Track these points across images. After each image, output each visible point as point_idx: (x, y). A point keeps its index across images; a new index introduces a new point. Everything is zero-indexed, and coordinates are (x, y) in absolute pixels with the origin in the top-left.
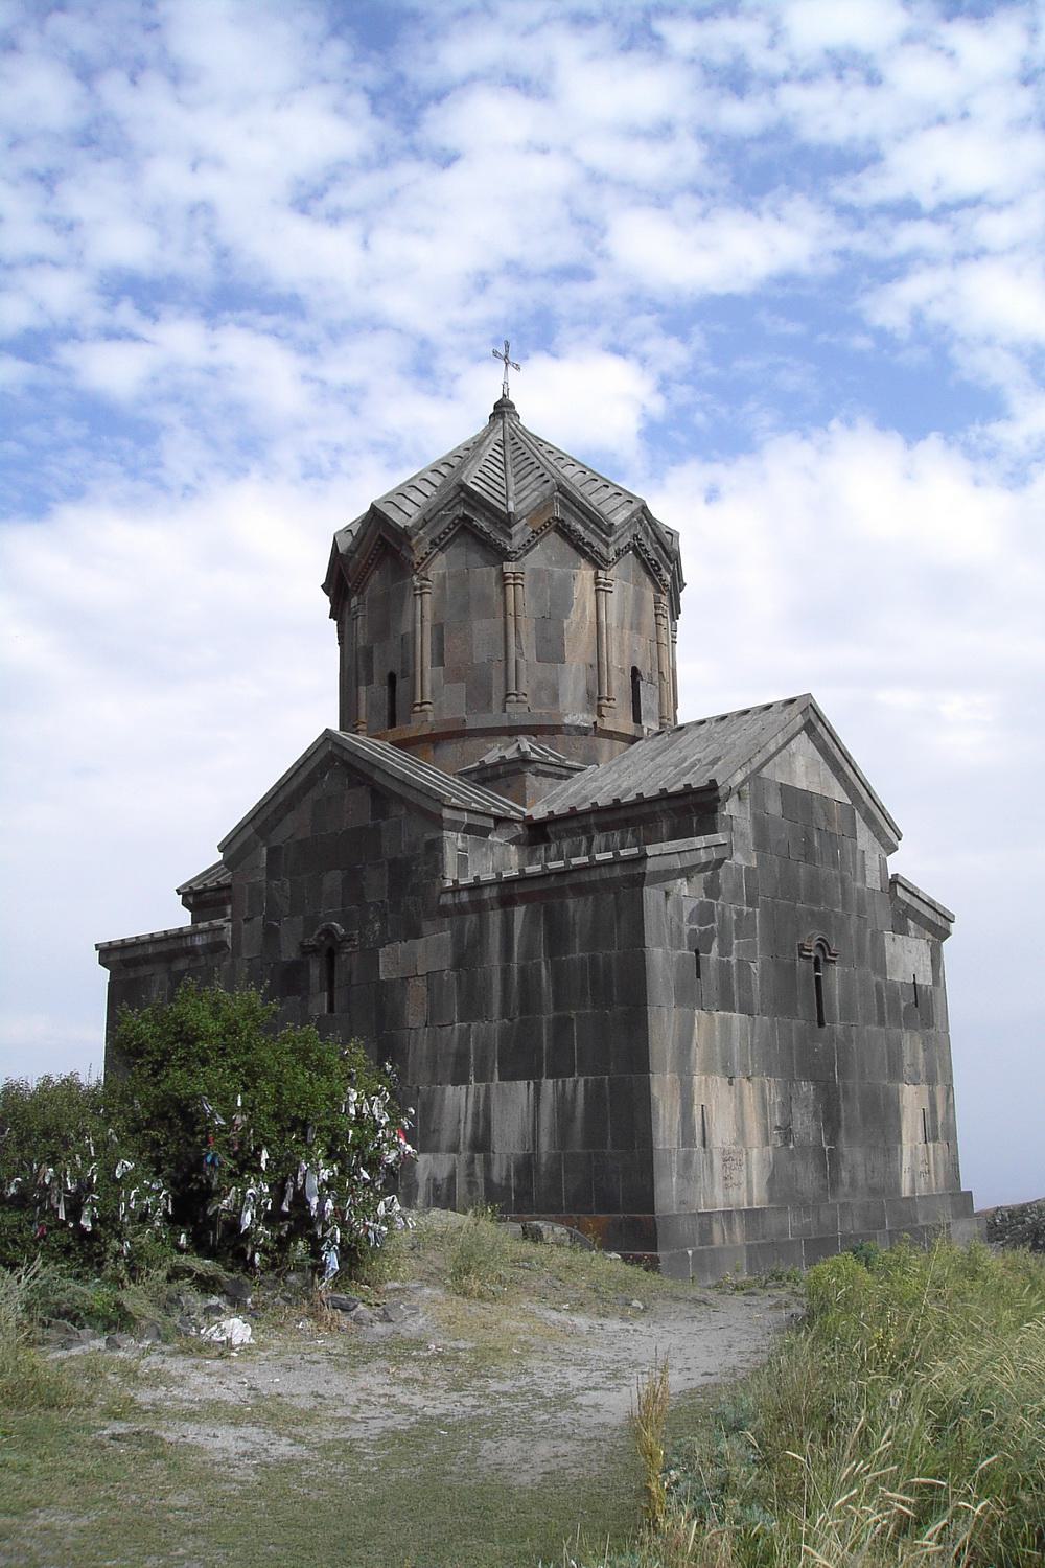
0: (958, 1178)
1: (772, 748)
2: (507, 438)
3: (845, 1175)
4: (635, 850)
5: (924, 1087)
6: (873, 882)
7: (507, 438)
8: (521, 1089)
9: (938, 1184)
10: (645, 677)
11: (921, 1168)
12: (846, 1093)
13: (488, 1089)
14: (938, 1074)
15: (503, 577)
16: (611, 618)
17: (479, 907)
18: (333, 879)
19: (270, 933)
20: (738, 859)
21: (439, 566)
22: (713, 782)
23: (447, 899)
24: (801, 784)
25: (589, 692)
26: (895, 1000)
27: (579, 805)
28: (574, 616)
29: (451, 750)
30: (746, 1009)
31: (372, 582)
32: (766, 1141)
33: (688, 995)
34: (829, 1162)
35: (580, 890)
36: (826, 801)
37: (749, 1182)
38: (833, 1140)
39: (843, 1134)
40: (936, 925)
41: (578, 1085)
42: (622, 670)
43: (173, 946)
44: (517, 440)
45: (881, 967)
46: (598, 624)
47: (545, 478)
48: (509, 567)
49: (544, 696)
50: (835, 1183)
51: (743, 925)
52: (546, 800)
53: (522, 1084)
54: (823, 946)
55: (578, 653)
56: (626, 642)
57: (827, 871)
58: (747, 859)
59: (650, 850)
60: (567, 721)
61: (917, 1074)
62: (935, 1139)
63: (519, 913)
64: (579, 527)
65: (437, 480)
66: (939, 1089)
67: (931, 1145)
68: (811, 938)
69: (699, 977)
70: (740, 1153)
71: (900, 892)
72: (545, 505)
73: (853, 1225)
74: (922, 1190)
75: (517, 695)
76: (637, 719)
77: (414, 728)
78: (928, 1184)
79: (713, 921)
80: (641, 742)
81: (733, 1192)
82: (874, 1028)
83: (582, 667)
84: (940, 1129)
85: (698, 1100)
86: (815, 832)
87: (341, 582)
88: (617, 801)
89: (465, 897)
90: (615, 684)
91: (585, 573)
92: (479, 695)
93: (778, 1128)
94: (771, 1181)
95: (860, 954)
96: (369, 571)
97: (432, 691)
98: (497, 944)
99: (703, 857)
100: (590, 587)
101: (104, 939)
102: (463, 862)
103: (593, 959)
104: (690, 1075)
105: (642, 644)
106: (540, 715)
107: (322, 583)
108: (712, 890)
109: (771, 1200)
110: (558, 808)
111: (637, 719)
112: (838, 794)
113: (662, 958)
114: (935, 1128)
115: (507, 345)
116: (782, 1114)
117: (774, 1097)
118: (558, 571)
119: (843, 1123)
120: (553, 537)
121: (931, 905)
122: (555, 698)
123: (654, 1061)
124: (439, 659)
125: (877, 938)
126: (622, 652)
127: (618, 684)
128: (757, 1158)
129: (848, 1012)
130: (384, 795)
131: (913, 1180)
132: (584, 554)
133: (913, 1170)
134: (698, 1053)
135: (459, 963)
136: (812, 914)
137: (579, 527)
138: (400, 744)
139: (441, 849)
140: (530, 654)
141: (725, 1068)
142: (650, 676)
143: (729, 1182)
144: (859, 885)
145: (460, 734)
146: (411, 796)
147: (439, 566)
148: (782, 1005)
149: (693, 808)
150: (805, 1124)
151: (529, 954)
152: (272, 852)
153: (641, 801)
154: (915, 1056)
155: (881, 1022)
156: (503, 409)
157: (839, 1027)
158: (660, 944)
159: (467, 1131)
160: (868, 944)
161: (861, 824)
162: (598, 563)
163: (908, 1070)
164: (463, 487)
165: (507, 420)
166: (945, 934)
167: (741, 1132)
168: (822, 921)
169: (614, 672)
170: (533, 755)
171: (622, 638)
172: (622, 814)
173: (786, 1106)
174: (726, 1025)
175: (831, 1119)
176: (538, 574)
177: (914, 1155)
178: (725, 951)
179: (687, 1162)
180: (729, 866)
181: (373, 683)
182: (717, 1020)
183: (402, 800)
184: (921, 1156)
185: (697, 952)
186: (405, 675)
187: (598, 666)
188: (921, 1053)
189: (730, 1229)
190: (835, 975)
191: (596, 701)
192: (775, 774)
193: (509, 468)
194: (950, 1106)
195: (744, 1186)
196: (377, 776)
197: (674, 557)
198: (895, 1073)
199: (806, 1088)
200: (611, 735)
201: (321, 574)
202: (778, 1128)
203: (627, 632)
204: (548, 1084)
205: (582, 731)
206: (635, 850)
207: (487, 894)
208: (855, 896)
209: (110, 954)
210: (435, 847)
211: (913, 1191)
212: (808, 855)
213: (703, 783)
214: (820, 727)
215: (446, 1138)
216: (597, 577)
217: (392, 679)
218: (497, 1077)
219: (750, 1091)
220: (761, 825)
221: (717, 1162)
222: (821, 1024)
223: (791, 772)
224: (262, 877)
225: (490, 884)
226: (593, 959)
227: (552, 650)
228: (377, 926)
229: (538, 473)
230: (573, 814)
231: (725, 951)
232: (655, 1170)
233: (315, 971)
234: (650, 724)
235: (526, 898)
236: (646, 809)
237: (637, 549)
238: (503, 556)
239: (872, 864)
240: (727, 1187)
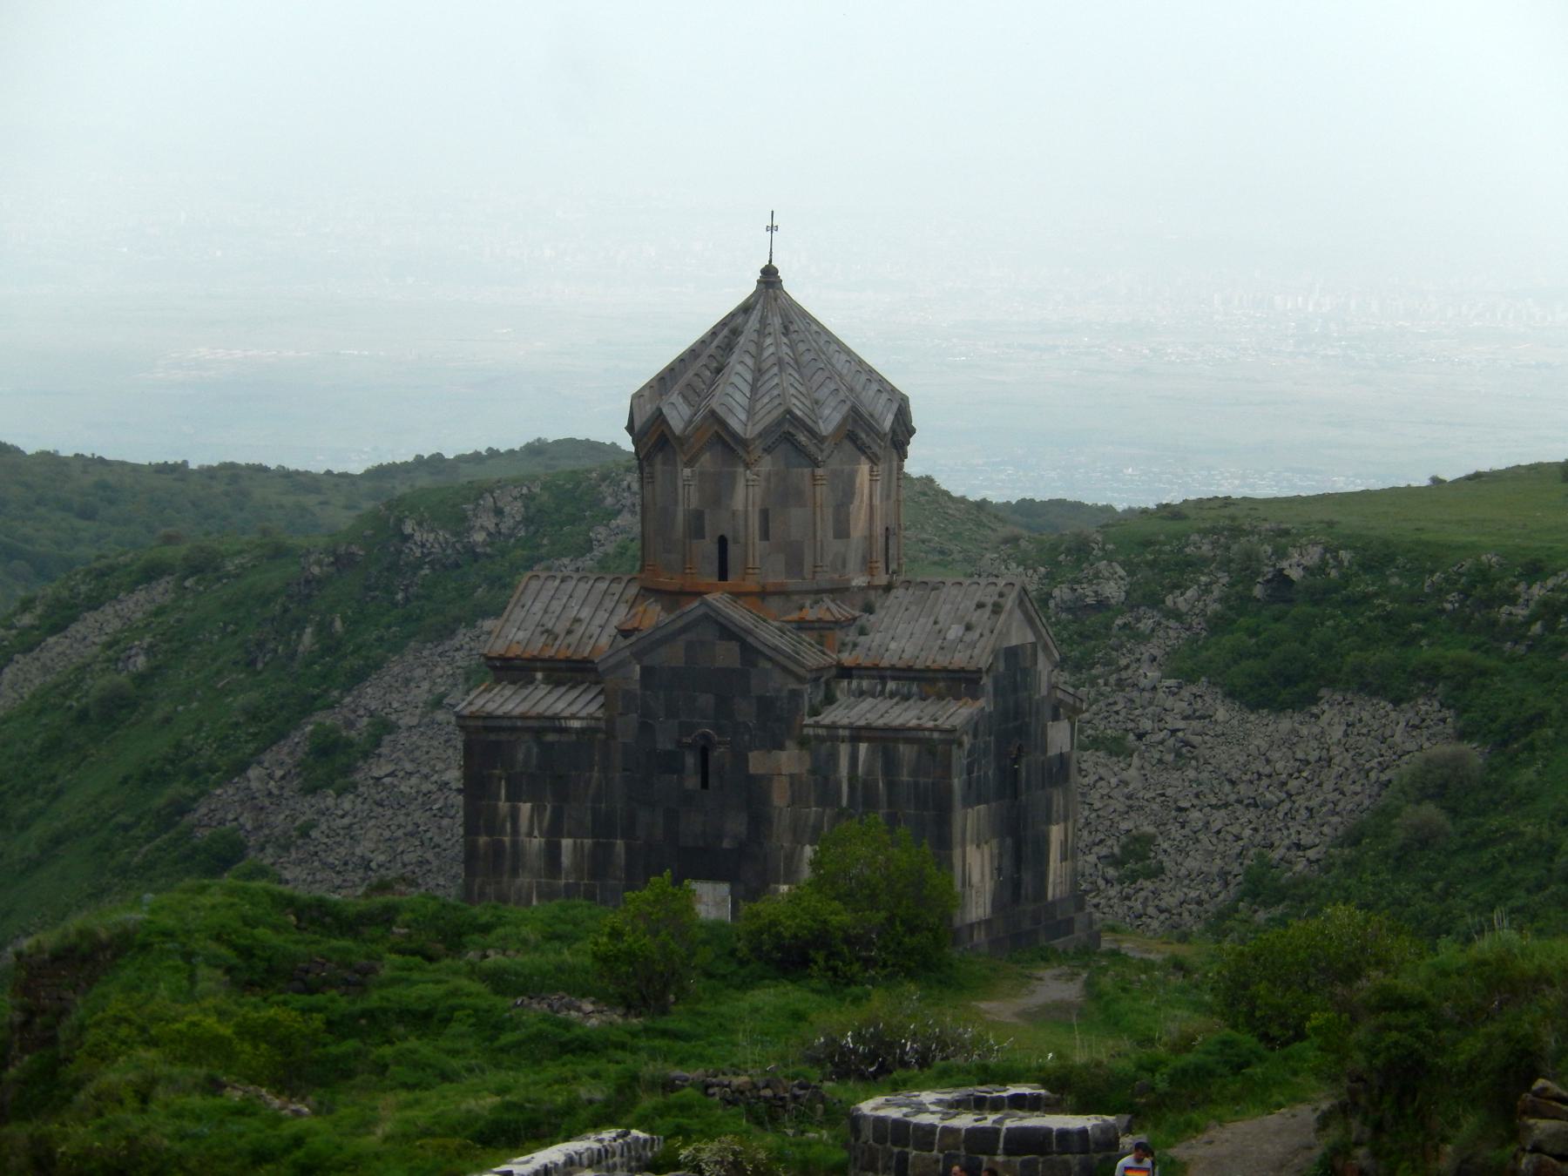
6: (1044, 692)
15: (813, 475)
16: (877, 501)
17: (835, 739)
18: (706, 700)
19: (645, 728)
21: (766, 465)
23: (806, 731)
24: (1014, 642)
28: (856, 502)
29: (774, 603)
30: (986, 802)
33: (967, 803)
34: (1017, 885)
35: (908, 741)
36: (1023, 646)
43: (547, 724)
45: (1045, 751)
46: (871, 506)
47: (842, 396)
48: (819, 472)
55: (858, 529)
60: (854, 583)
63: (863, 747)
72: (845, 419)
77: (751, 584)
89: (821, 731)
91: (864, 468)
92: (794, 563)
100: (866, 477)
103: (916, 784)
108: (975, 736)
112: (1031, 638)
113: (957, 783)
117: (996, 851)
118: (847, 468)
120: (848, 445)
122: (844, 565)
124: (765, 535)
125: (1045, 726)
128: (989, 885)
132: (864, 453)
135: (813, 771)
137: (863, 435)
138: (737, 595)
140: (831, 534)
145: (783, 593)
146: (780, 658)
147: (766, 465)
151: (870, 771)
152: (647, 672)
153: (928, 669)
156: (769, 277)
161: (1041, 655)
162: (874, 459)
163: (1054, 815)
167: (983, 875)
172: (912, 675)
173: (1001, 855)
175: (1018, 860)
181: (703, 537)
183: (770, 659)
186: (736, 541)
187: (870, 538)
191: (868, 566)
196: (750, 639)
199: (1009, 841)
200: (876, 588)
205: (861, 589)
207: (841, 732)
213: (972, 667)
216: (871, 471)
217: (723, 542)
219: (986, 848)
224: (636, 687)
225: (844, 727)
226: (916, 784)
227: (842, 532)
228: (747, 737)
229: (833, 386)
230: (876, 667)
233: (691, 760)
235: (868, 740)
236: (930, 675)
238: (816, 464)
239: (1044, 678)
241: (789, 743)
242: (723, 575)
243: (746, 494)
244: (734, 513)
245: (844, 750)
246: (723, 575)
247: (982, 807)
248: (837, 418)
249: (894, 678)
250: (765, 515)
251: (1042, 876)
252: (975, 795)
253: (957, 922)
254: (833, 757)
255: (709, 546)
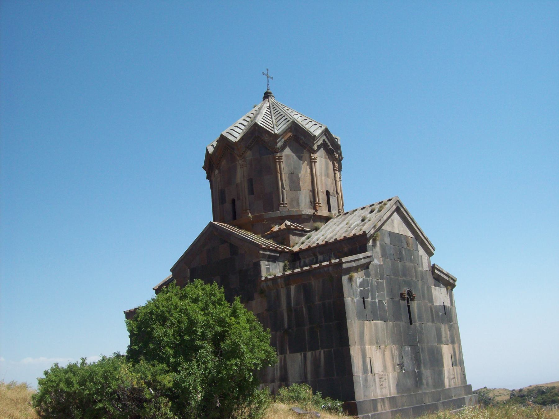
0: (465, 379)
1: (385, 218)
2: (271, 105)
3: (424, 381)
4: (337, 260)
5: (450, 345)
6: (426, 267)
7: (271, 105)
8: (299, 357)
9: (459, 383)
10: (331, 194)
11: (452, 377)
12: (422, 350)
13: (285, 357)
14: (455, 340)
20: (376, 262)
22: (364, 232)
24: (397, 232)
25: (311, 201)
26: (437, 313)
27: (330, 239)
31: (223, 163)
32: (394, 370)
37: (389, 387)
38: (419, 368)
39: (422, 365)
40: (449, 284)
41: (322, 353)
42: (323, 192)
44: (275, 106)
45: (431, 300)
49: (295, 203)
50: (421, 383)
51: (379, 287)
52: (298, 244)
53: (299, 354)
54: (409, 293)
55: (305, 186)
56: (323, 181)
57: (409, 264)
58: (379, 261)
59: (344, 260)
60: (303, 213)
61: (448, 340)
62: (456, 365)
63: (293, 288)
64: (303, 138)
65: (245, 123)
66: (456, 346)
67: (455, 367)
68: (405, 290)
69: (365, 308)
70: (385, 375)
71: (436, 271)
73: (428, 401)
74: (453, 385)
75: (283, 204)
76: (330, 210)
78: (455, 383)
79: (368, 286)
80: (331, 220)
81: (384, 390)
82: (430, 324)
83: (308, 192)
84: (458, 361)
85: (368, 356)
86: (403, 249)
87: (212, 164)
88: (326, 242)
90: (320, 197)
93: (398, 365)
94: (397, 385)
95: (423, 296)
96: (220, 161)
97: (250, 205)
98: (282, 299)
99: (363, 261)
101: (127, 309)
102: (268, 270)
104: (364, 346)
105: (330, 181)
106: (293, 211)
107: (203, 165)
109: (398, 392)
110: (304, 247)
111: (330, 210)
112: (410, 234)
113: (351, 302)
114: (456, 360)
115: (268, 70)
116: (399, 359)
117: (396, 353)
119: (422, 361)
121: (447, 275)
122: (298, 204)
123: (351, 342)
124: (251, 192)
126: (322, 185)
127: (322, 197)
129: (420, 317)
130: (235, 246)
131: (449, 381)
133: (449, 378)
134: (367, 338)
136: (404, 281)
137: (303, 138)
139: (259, 265)
140: (287, 188)
141: (377, 343)
142: (333, 193)
143: (382, 387)
144: (421, 269)
147: (249, 154)
148: (397, 317)
149: (357, 243)
150: (407, 362)
154: (446, 334)
155: (433, 321)
157: (418, 324)
158: (349, 296)
159: (278, 374)
160: (426, 292)
163: (444, 339)
164: (256, 124)
165: (270, 99)
166: (453, 286)
167: (385, 367)
168: (408, 284)
169: (320, 194)
170: (292, 227)
171: (321, 179)
174: (375, 324)
175: (417, 360)
176: (287, 156)
177: (449, 372)
178: (373, 297)
179: (366, 380)
180: (373, 265)
182: (373, 324)
184: (451, 372)
185: (363, 299)
186: (238, 199)
187: (313, 191)
188: (448, 333)
189: (384, 405)
190: (414, 305)
191: (314, 204)
192: (387, 228)
193: (273, 117)
194: (461, 352)
195: (388, 388)
197: (337, 148)
198: (440, 341)
199: (408, 348)
201: (202, 163)
202: (398, 365)
203: (323, 178)
204: (309, 354)
206: (337, 260)
208: (419, 273)
209: (130, 315)
210: (257, 266)
211: (450, 386)
212: (401, 259)
213: (361, 232)
214: (402, 209)
215: (270, 377)
217: (234, 201)
218: (288, 352)
220: (383, 248)
221: (377, 379)
222: (411, 323)
223: (393, 226)
231: (373, 297)
232: (355, 384)
234: (334, 212)
237: (324, 145)
240: (381, 389)
241: (256, 296)
242: (235, 218)
243: (241, 175)
244: (237, 185)
245: (283, 292)
246: (235, 218)
247: (380, 323)
248: (285, 126)
249: (321, 253)
250: (250, 182)
251: (440, 374)
252: (370, 311)
253: (360, 395)
254: (278, 296)
255: (228, 206)
